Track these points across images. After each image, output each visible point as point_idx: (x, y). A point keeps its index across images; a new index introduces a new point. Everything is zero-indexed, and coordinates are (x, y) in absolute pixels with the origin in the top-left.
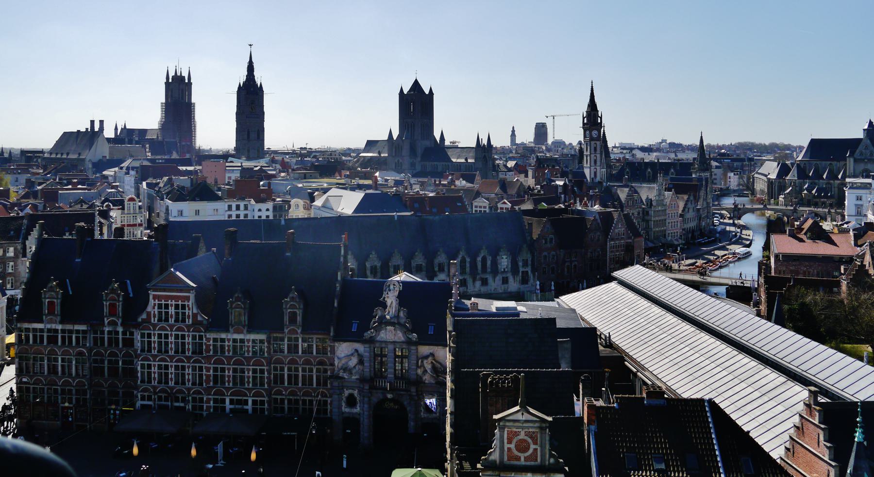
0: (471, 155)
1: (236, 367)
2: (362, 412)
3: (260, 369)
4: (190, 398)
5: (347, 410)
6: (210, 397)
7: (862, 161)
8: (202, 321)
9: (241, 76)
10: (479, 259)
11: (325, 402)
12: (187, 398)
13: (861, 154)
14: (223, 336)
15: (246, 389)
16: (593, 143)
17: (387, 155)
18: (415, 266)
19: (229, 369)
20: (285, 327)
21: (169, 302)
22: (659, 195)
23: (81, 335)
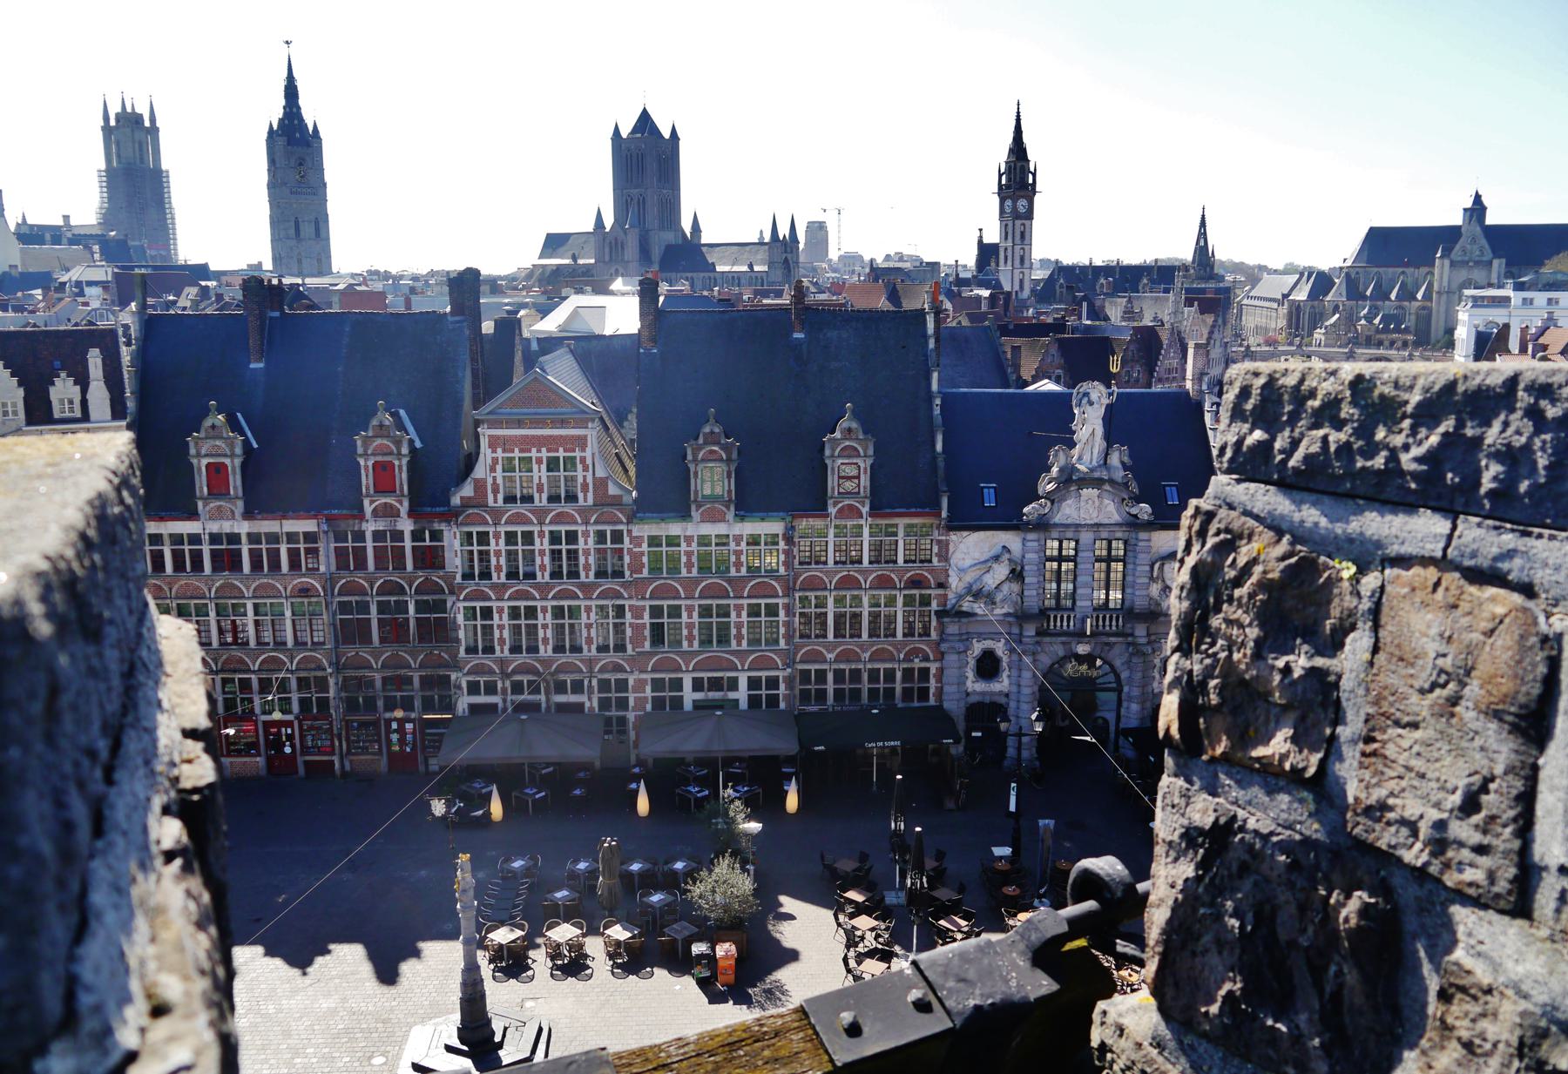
0: (759, 257)
1: (709, 602)
2: (1014, 689)
3: (766, 605)
4: (595, 682)
5: (980, 686)
7: (1464, 263)
8: (621, 496)
12: (586, 683)
13: (1464, 251)
15: (733, 653)
16: (1018, 222)
17: (592, 261)
19: (690, 609)
20: (830, 502)
21: (534, 453)
22: (1175, 313)
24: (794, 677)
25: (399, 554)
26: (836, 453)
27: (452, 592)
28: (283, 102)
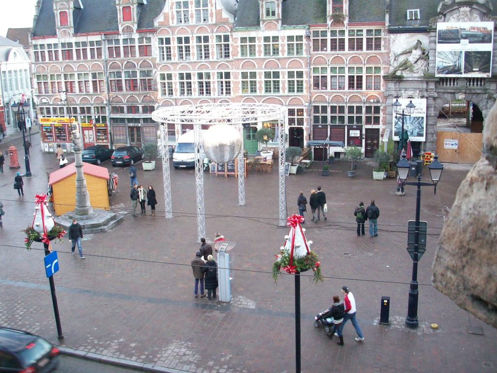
8: (228, 19)
11: (377, 110)
14: (253, 34)
15: (280, 96)
24: (311, 110)
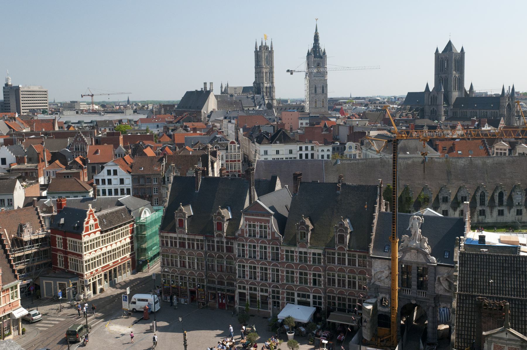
6: (284, 290)
9: (310, 46)
10: (497, 194)
14: (293, 249)
15: (308, 287)
18: (442, 198)
19: (297, 272)
20: (336, 245)
21: (256, 223)
23: (200, 243)
25: (222, 247)
26: (338, 231)
27: (235, 260)
28: (313, 42)
